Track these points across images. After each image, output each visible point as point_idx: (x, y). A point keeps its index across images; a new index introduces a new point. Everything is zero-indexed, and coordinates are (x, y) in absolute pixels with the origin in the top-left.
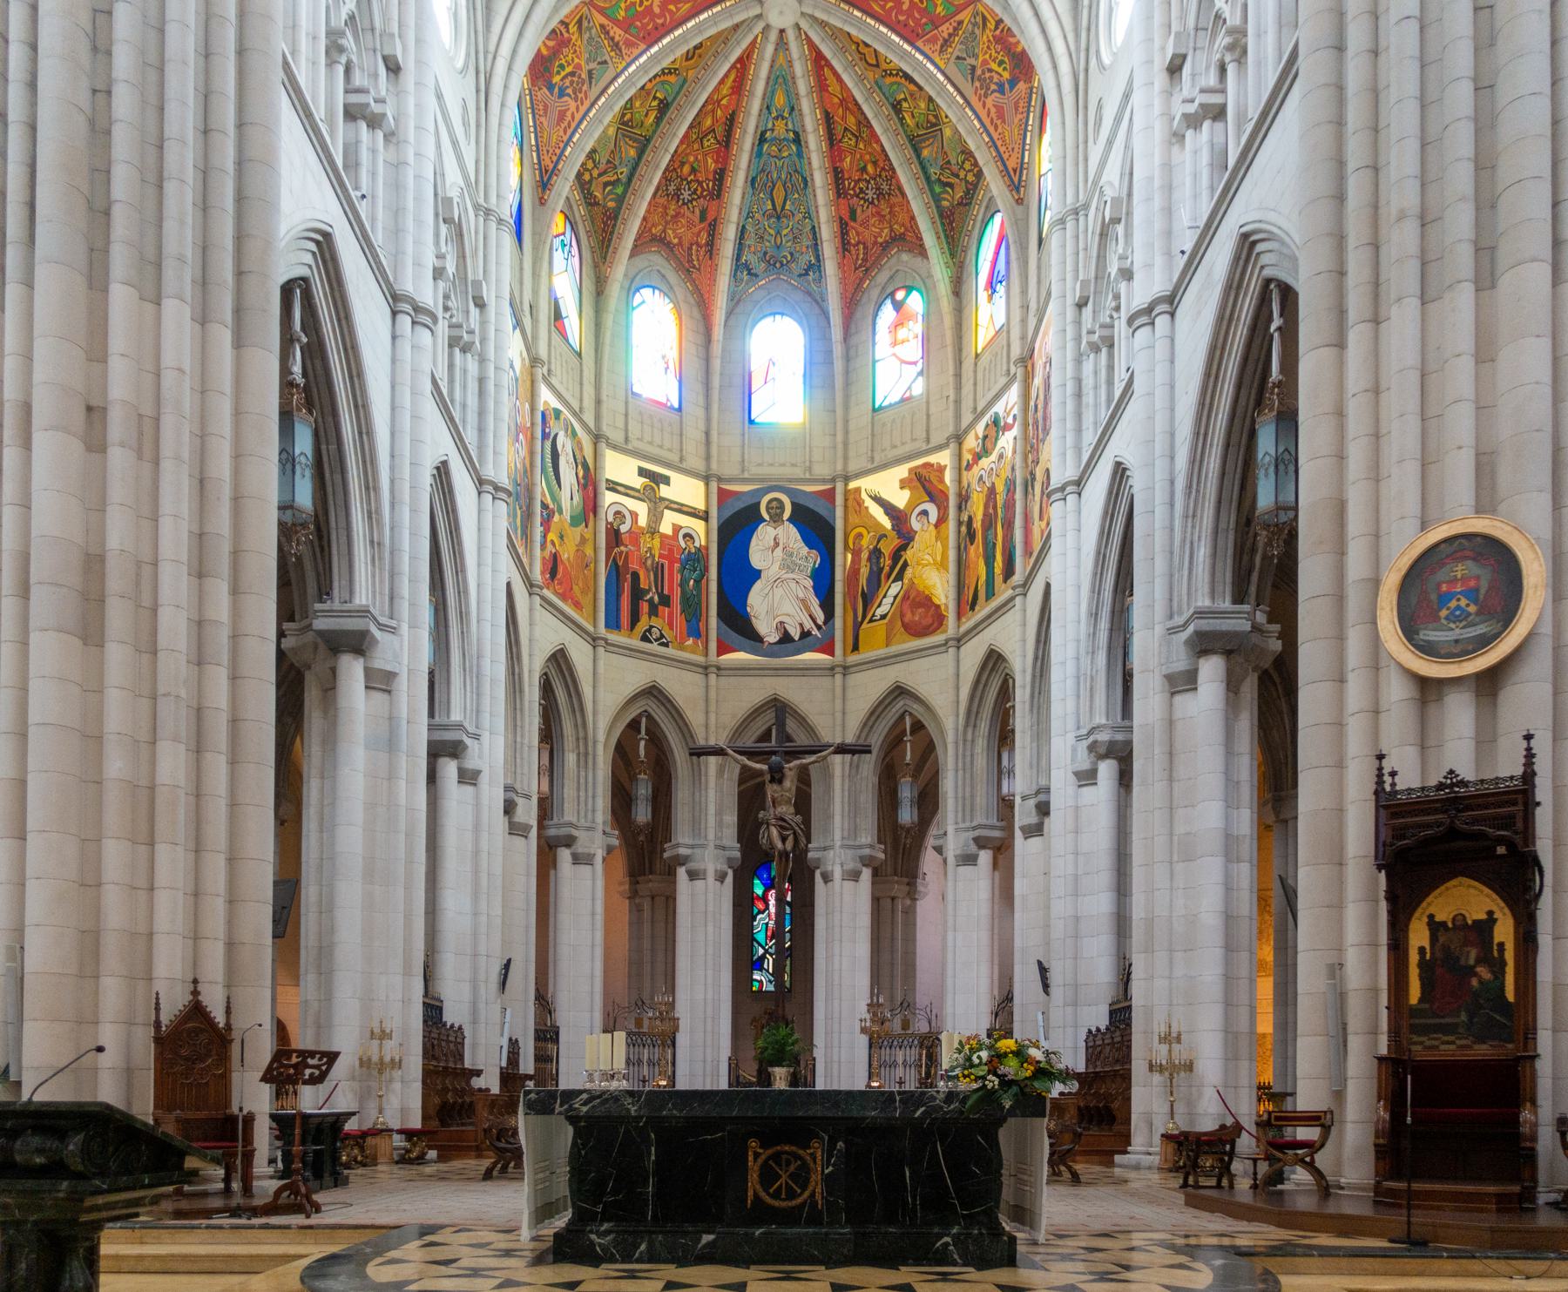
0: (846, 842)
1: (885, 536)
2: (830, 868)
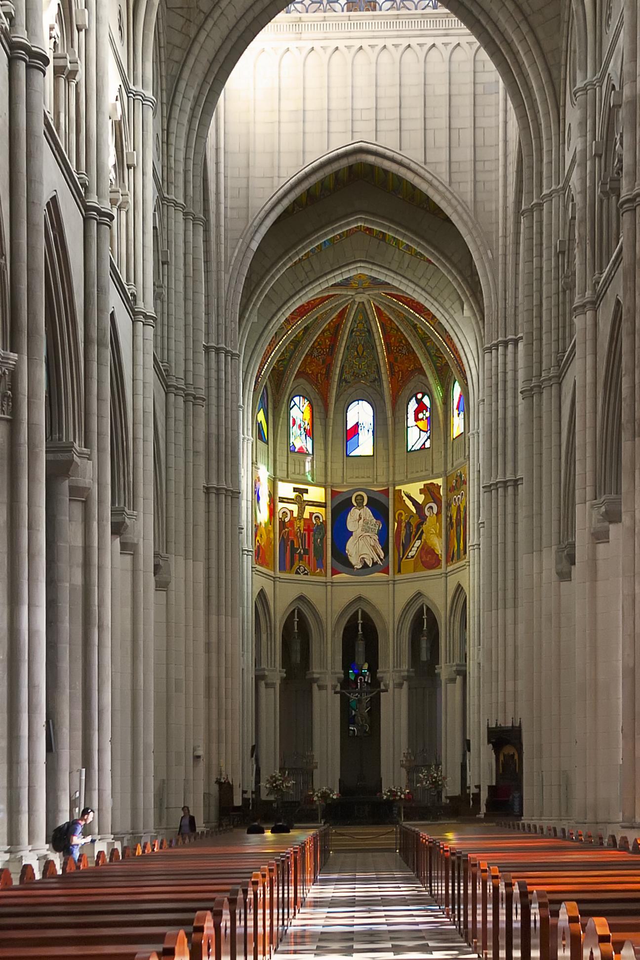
0: (395, 669)
1: (413, 516)
2: (388, 682)
